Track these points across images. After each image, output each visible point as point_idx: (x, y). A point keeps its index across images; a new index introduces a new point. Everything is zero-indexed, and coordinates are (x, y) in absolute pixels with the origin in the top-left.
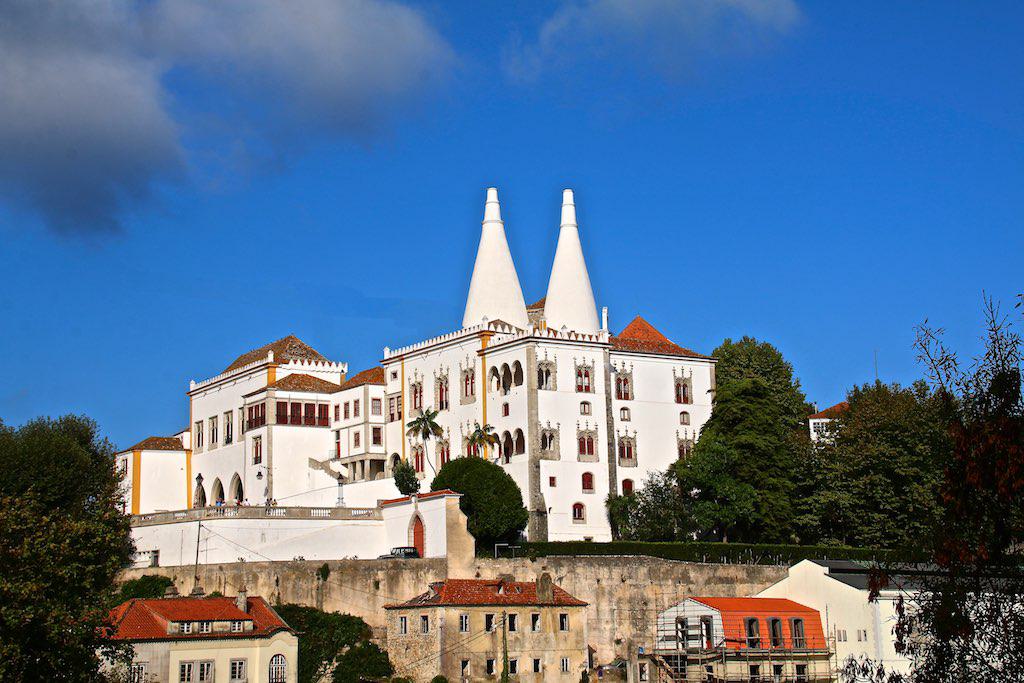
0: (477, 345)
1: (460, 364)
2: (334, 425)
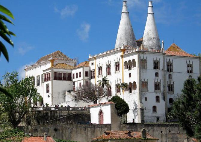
0: (121, 54)
1: (115, 60)
2: (74, 80)
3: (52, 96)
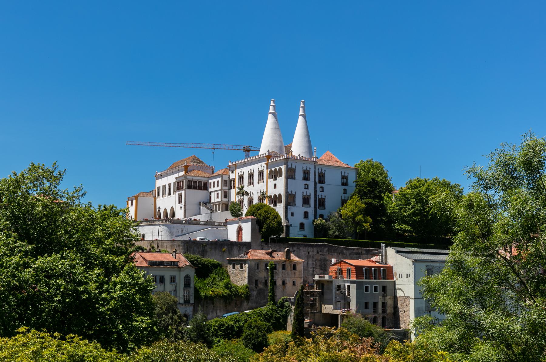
2: (210, 190)
3: (185, 208)
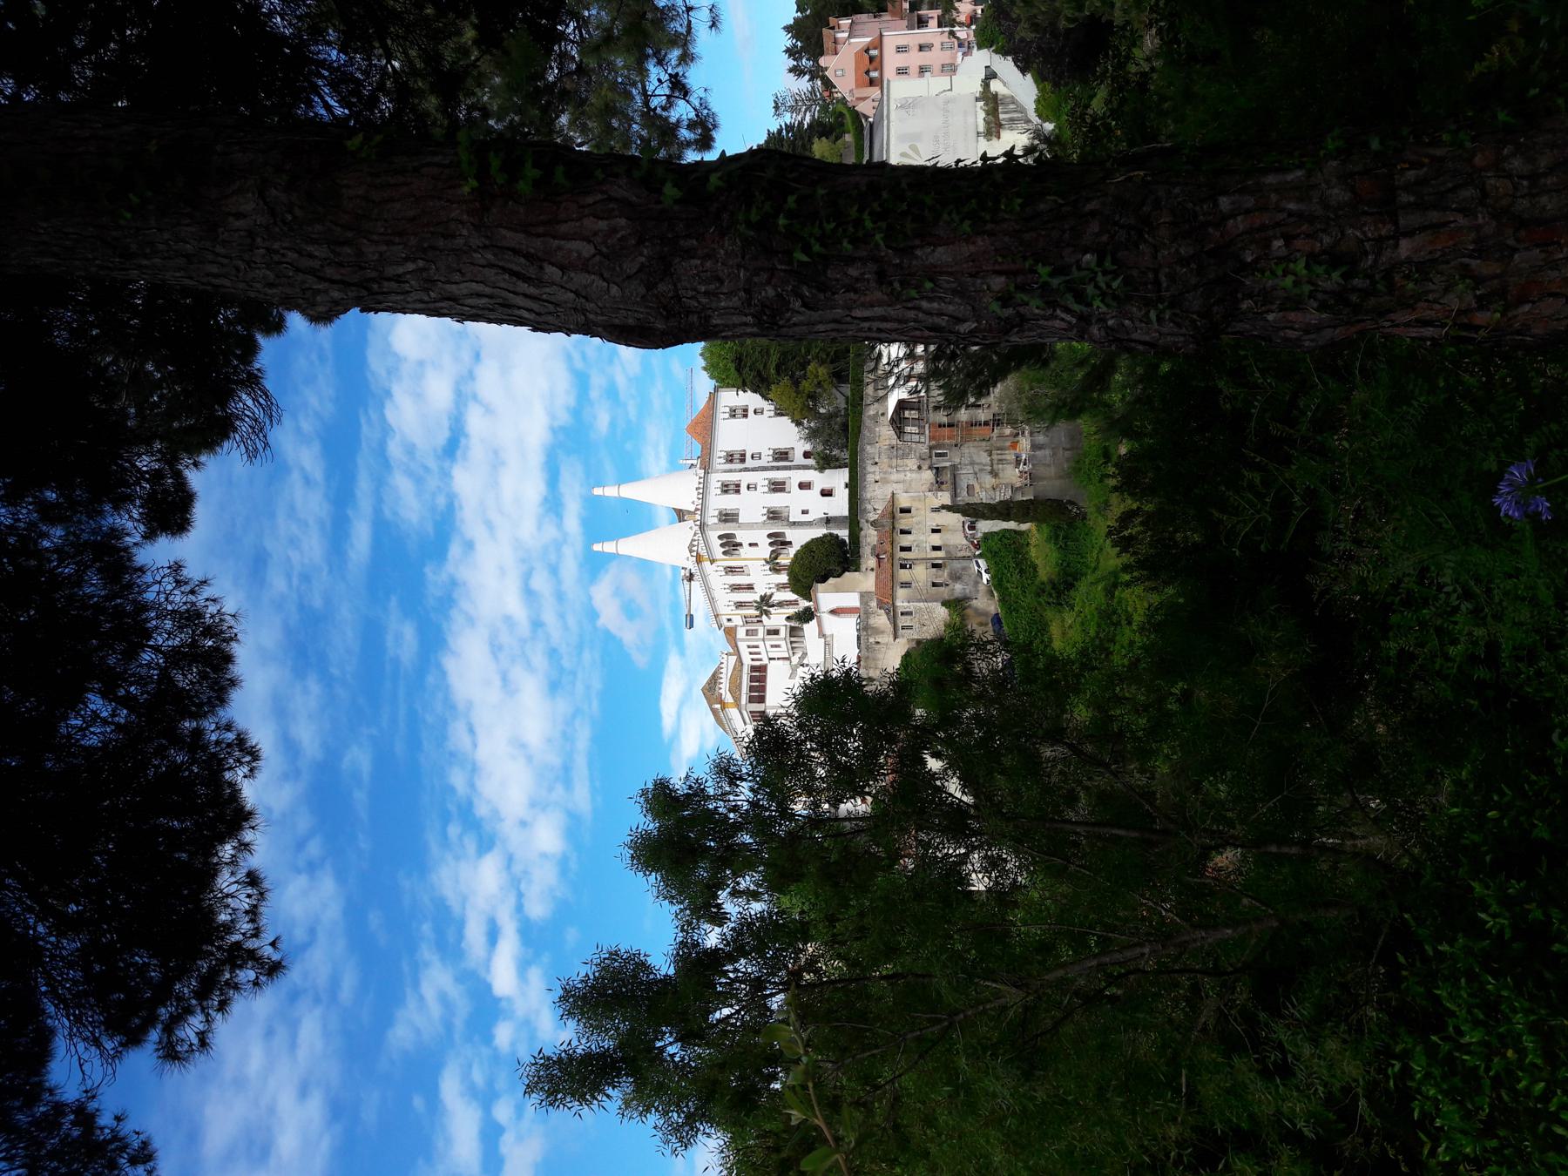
0: (706, 564)
2: (766, 661)
